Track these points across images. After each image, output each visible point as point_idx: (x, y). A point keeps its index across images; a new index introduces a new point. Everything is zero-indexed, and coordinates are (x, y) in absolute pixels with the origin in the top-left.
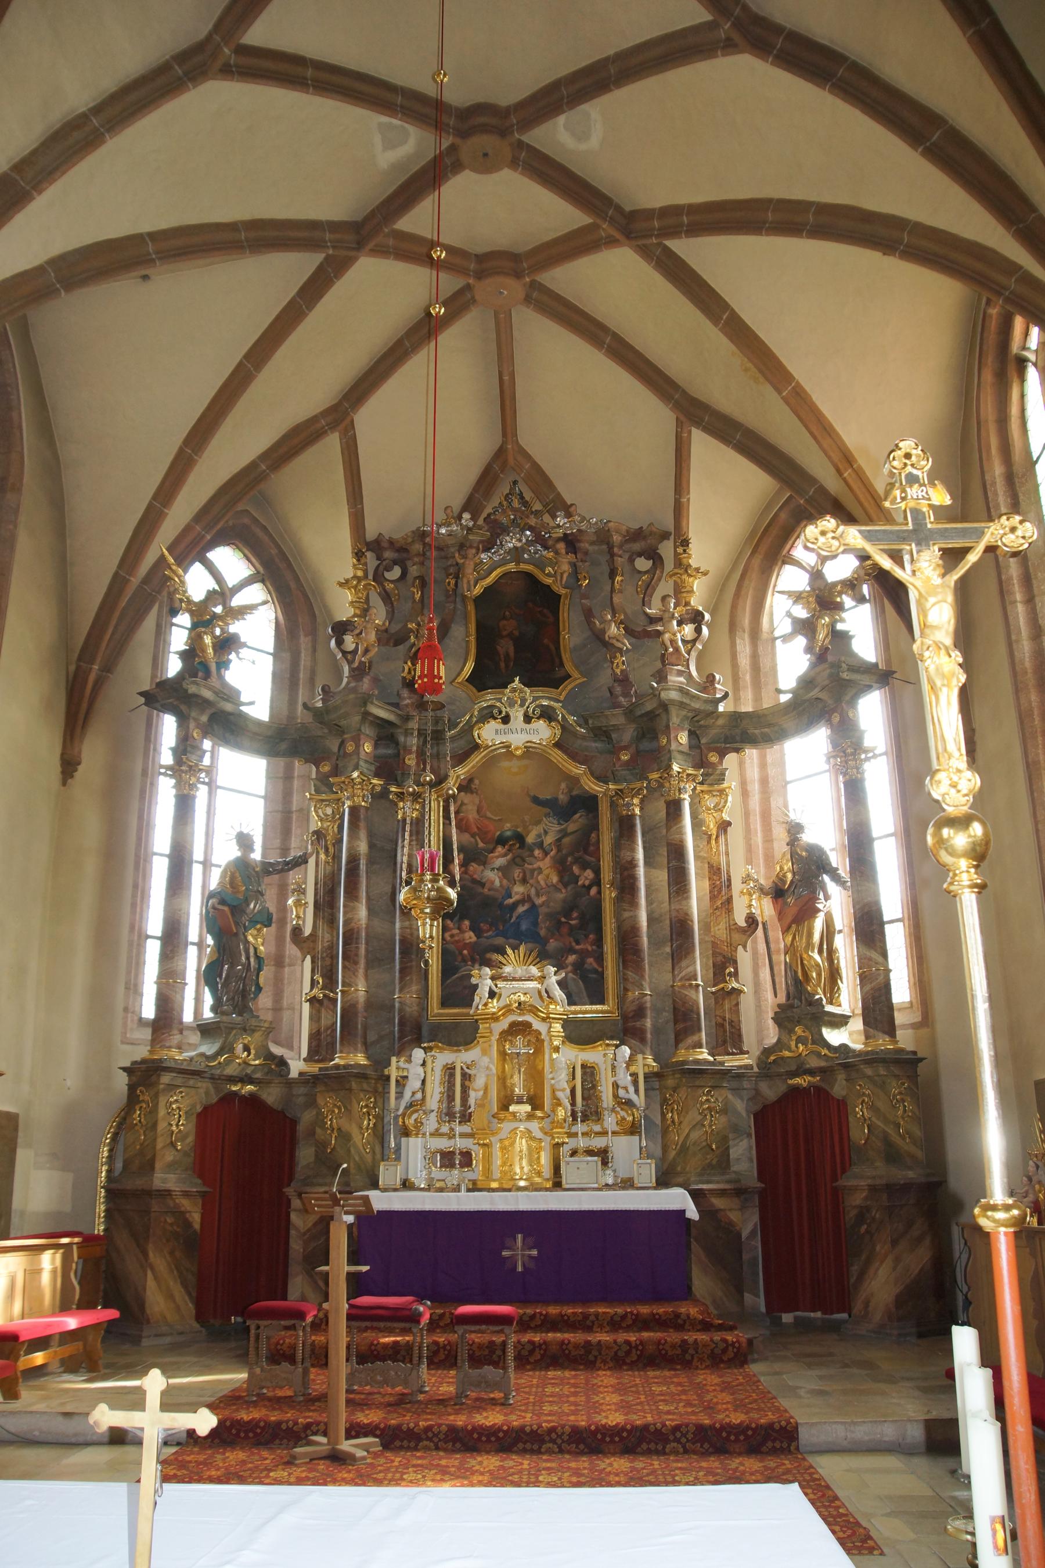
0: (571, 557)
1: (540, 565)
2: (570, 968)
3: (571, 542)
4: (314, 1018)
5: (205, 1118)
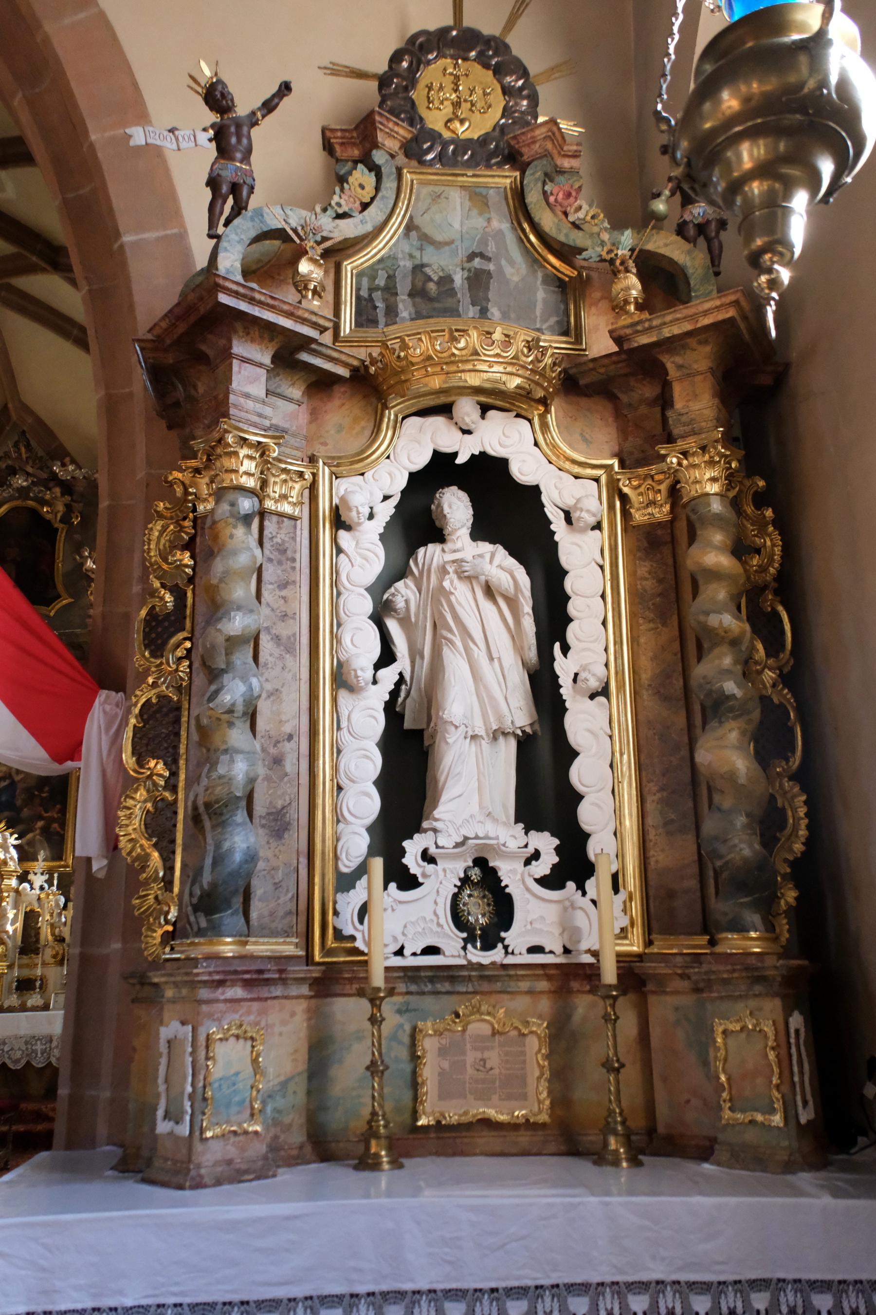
0: (68, 498)
1: (43, 502)
2: (38, 832)
3: (67, 487)
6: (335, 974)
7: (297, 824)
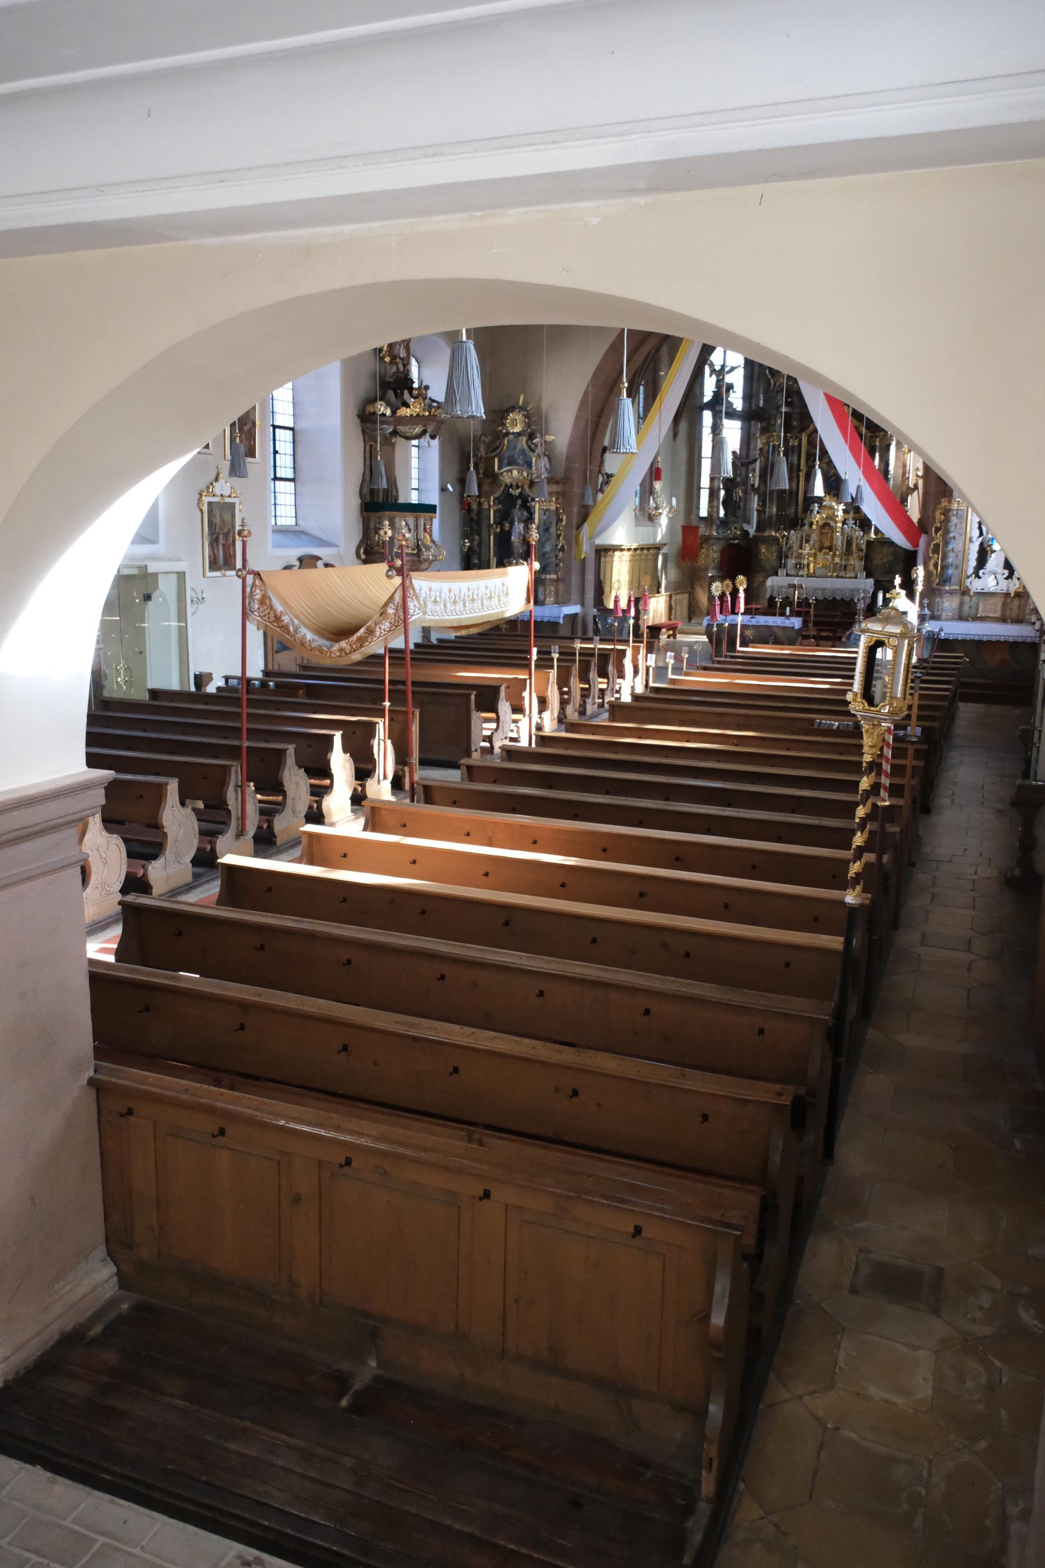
4: (759, 516)
5: (723, 552)
6: (965, 592)
7: (960, 567)
